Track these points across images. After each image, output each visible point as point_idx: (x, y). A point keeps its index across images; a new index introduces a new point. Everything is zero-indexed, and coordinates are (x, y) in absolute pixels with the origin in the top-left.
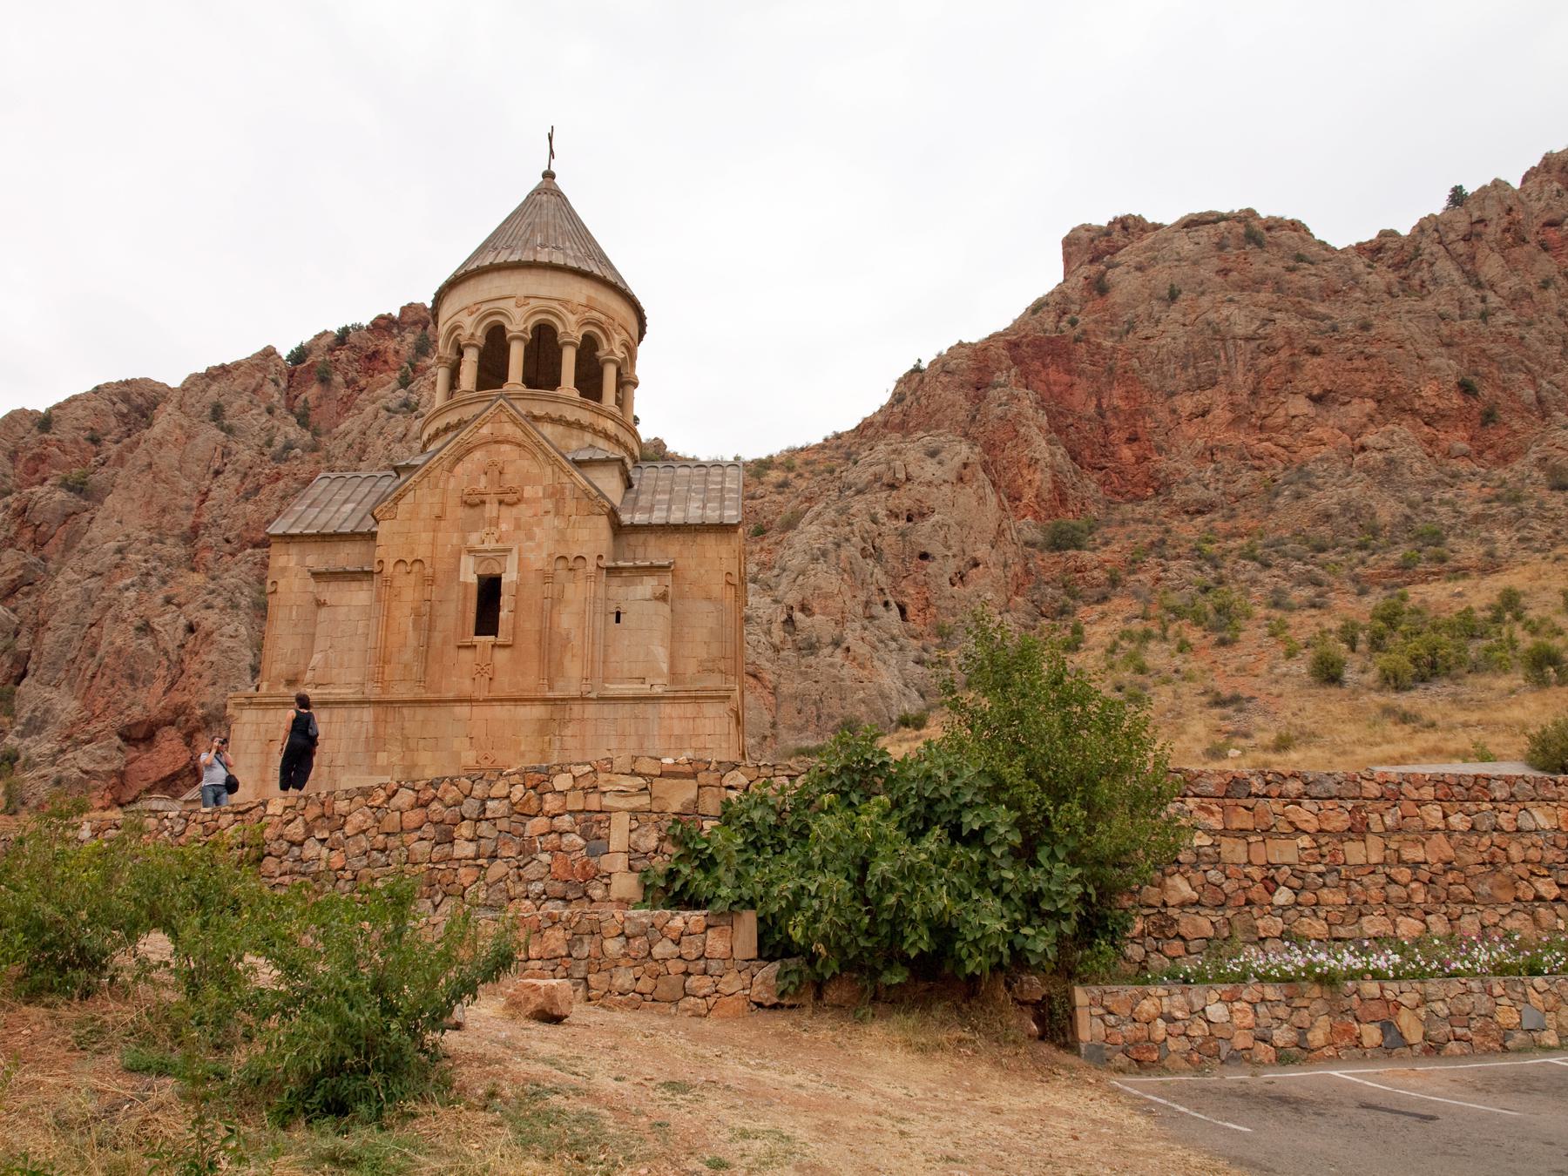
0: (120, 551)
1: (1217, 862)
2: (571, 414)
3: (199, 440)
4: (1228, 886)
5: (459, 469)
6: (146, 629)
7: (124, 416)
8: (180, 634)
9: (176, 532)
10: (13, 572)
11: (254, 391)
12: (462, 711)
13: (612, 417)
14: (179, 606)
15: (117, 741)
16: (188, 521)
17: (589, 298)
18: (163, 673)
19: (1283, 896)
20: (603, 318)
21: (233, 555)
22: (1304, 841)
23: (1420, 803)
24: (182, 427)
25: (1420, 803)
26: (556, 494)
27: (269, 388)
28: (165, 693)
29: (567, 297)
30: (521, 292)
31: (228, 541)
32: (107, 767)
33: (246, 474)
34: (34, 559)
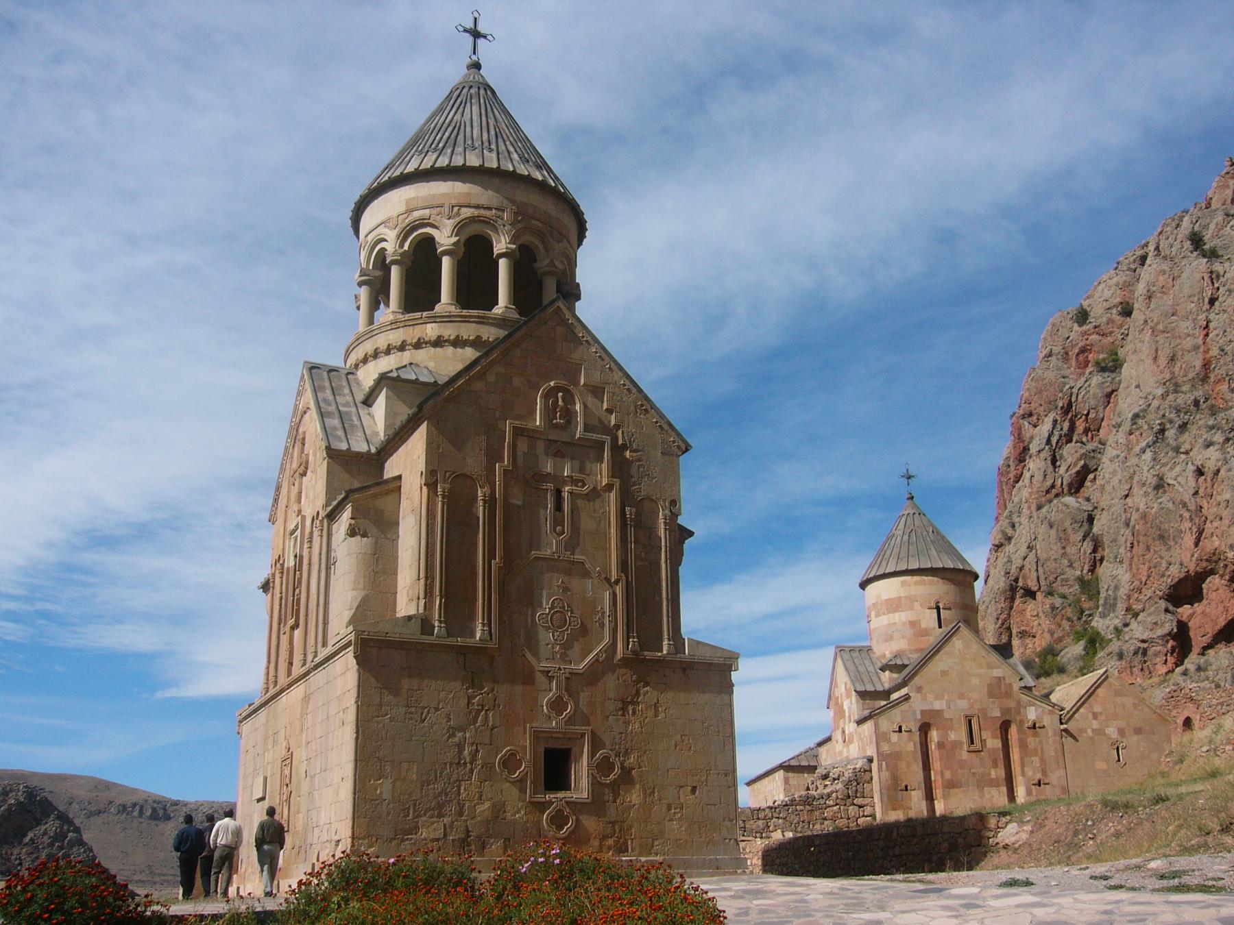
0: (1136, 416)
3: (1184, 275)
6: (1160, 485)
8: (1192, 482)
9: (1191, 375)
10: (1076, 464)
12: (284, 699)
14: (1187, 453)
15: (1163, 604)
16: (1198, 364)
17: (407, 202)
18: (1187, 525)
20: (427, 212)
28: (1196, 545)
32: (1160, 632)
34: (1090, 446)
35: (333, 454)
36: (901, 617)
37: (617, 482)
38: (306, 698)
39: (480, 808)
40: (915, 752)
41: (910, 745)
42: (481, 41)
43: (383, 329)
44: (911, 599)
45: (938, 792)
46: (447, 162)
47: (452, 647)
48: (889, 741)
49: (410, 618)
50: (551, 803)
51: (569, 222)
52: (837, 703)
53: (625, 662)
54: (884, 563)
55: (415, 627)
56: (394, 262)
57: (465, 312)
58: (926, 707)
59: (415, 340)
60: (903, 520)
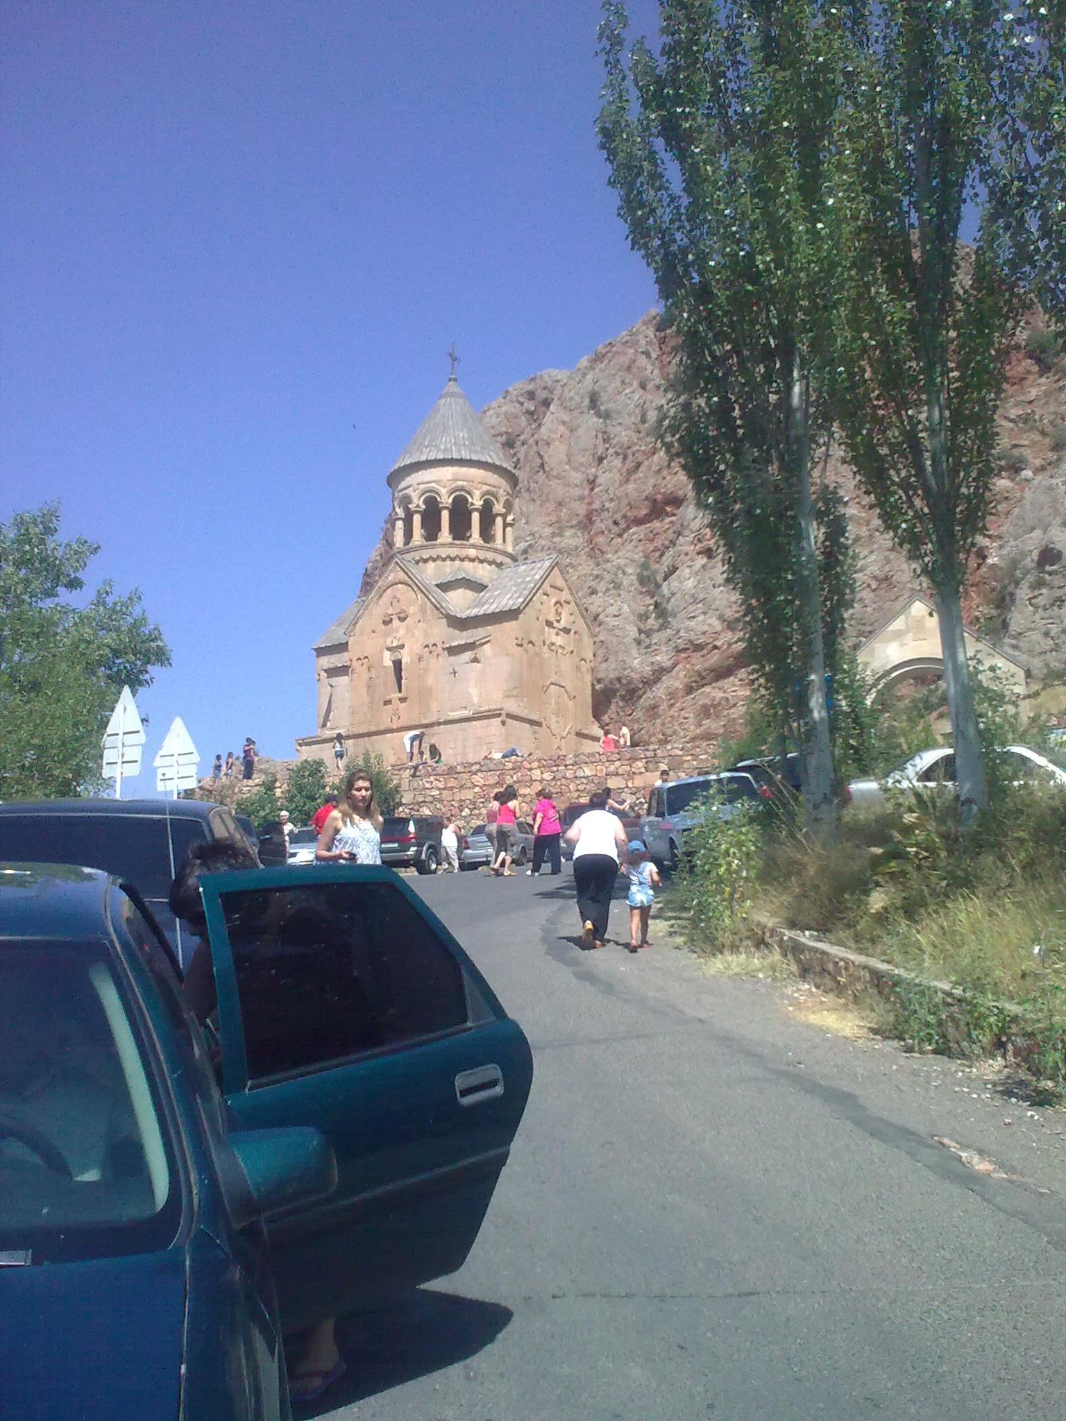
1: (441, 801)
2: (443, 552)
3: (581, 431)
4: (444, 809)
5: (380, 602)
7: (531, 413)
9: (574, 522)
11: (629, 368)
13: (473, 546)
19: (466, 812)
21: (620, 536)
22: (477, 790)
23: (530, 770)
24: (564, 423)
25: (530, 770)
26: (423, 610)
27: (642, 360)
30: (414, 483)
31: (616, 523)
33: (625, 458)
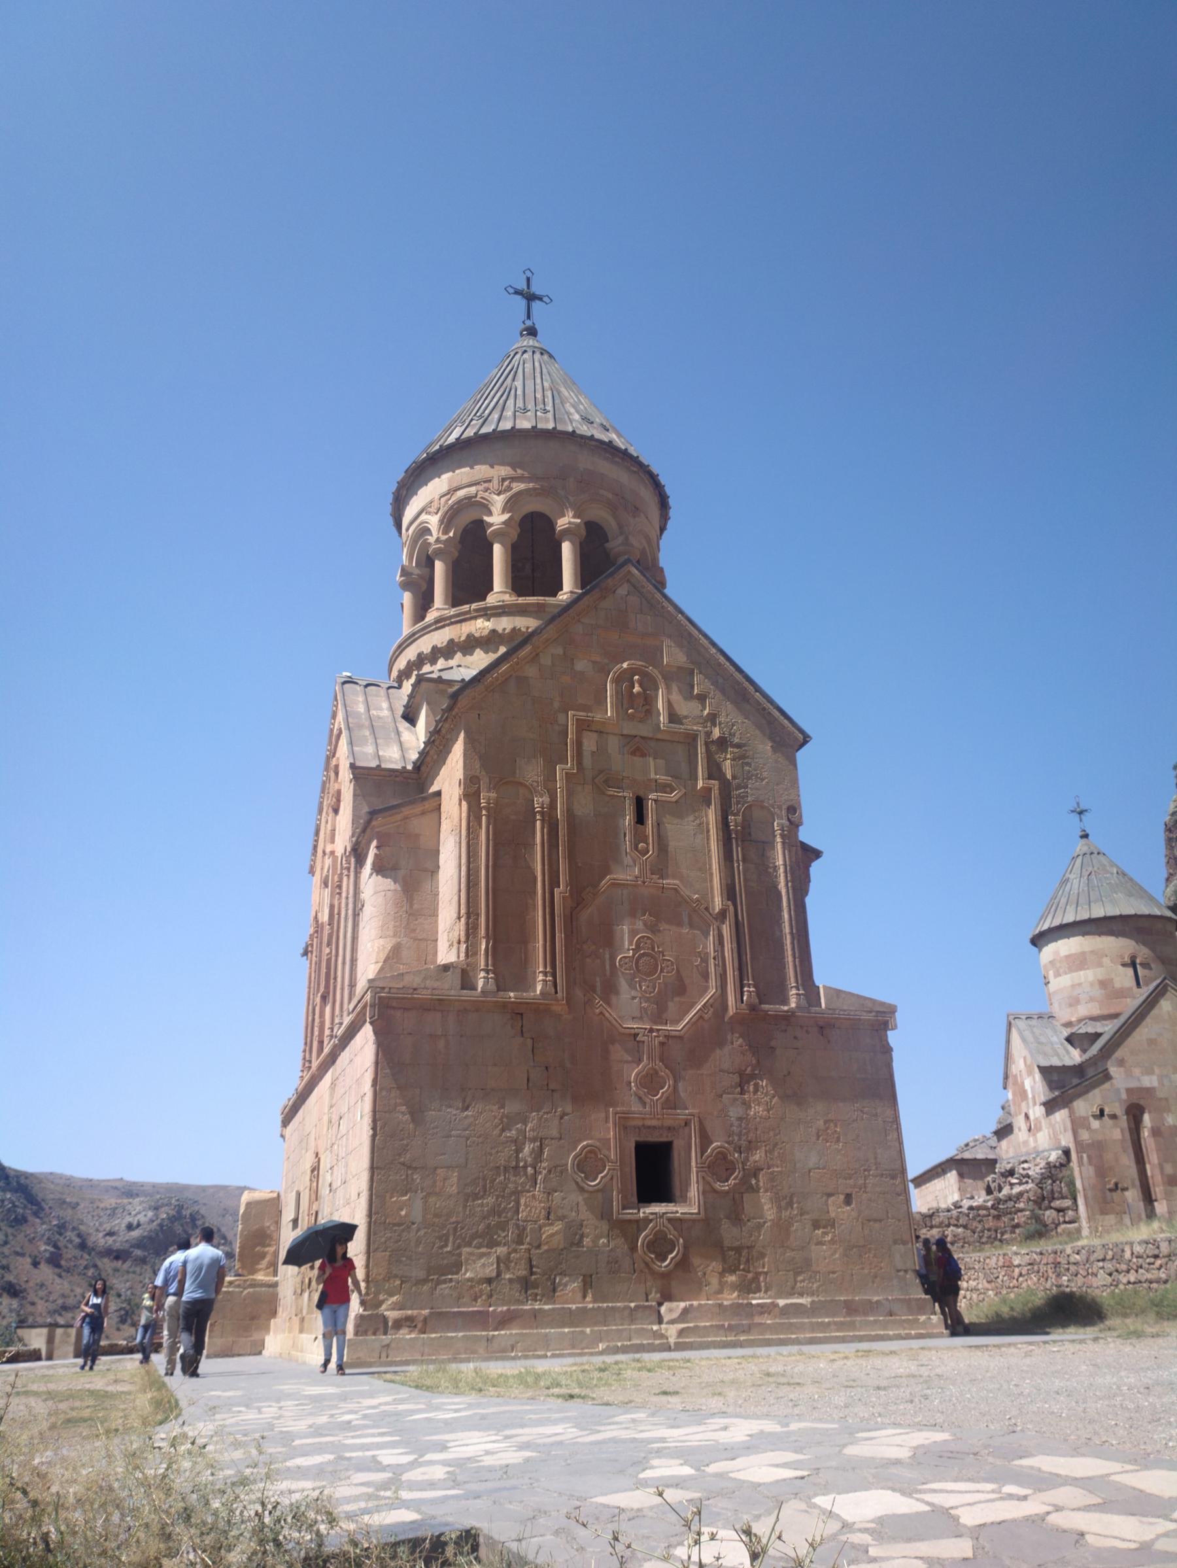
17: (450, 480)
20: (473, 490)
29: (428, 500)
35: (360, 774)
36: (1088, 976)
37: (715, 784)
38: (333, 1084)
39: (549, 1230)
40: (1123, 1140)
41: (1116, 1133)
42: (536, 305)
43: (426, 630)
44: (1098, 955)
45: (1158, 1190)
46: (493, 427)
47: (504, 1006)
48: (1088, 1128)
49: (446, 968)
50: (647, 1221)
51: (647, 495)
52: (1015, 1083)
53: (739, 1019)
54: (1059, 913)
55: (453, 979)
56: (439, 553)
57: (521, 600)
58: (1133, 1084)
59: (463, 638)
60: (1079, 861)
